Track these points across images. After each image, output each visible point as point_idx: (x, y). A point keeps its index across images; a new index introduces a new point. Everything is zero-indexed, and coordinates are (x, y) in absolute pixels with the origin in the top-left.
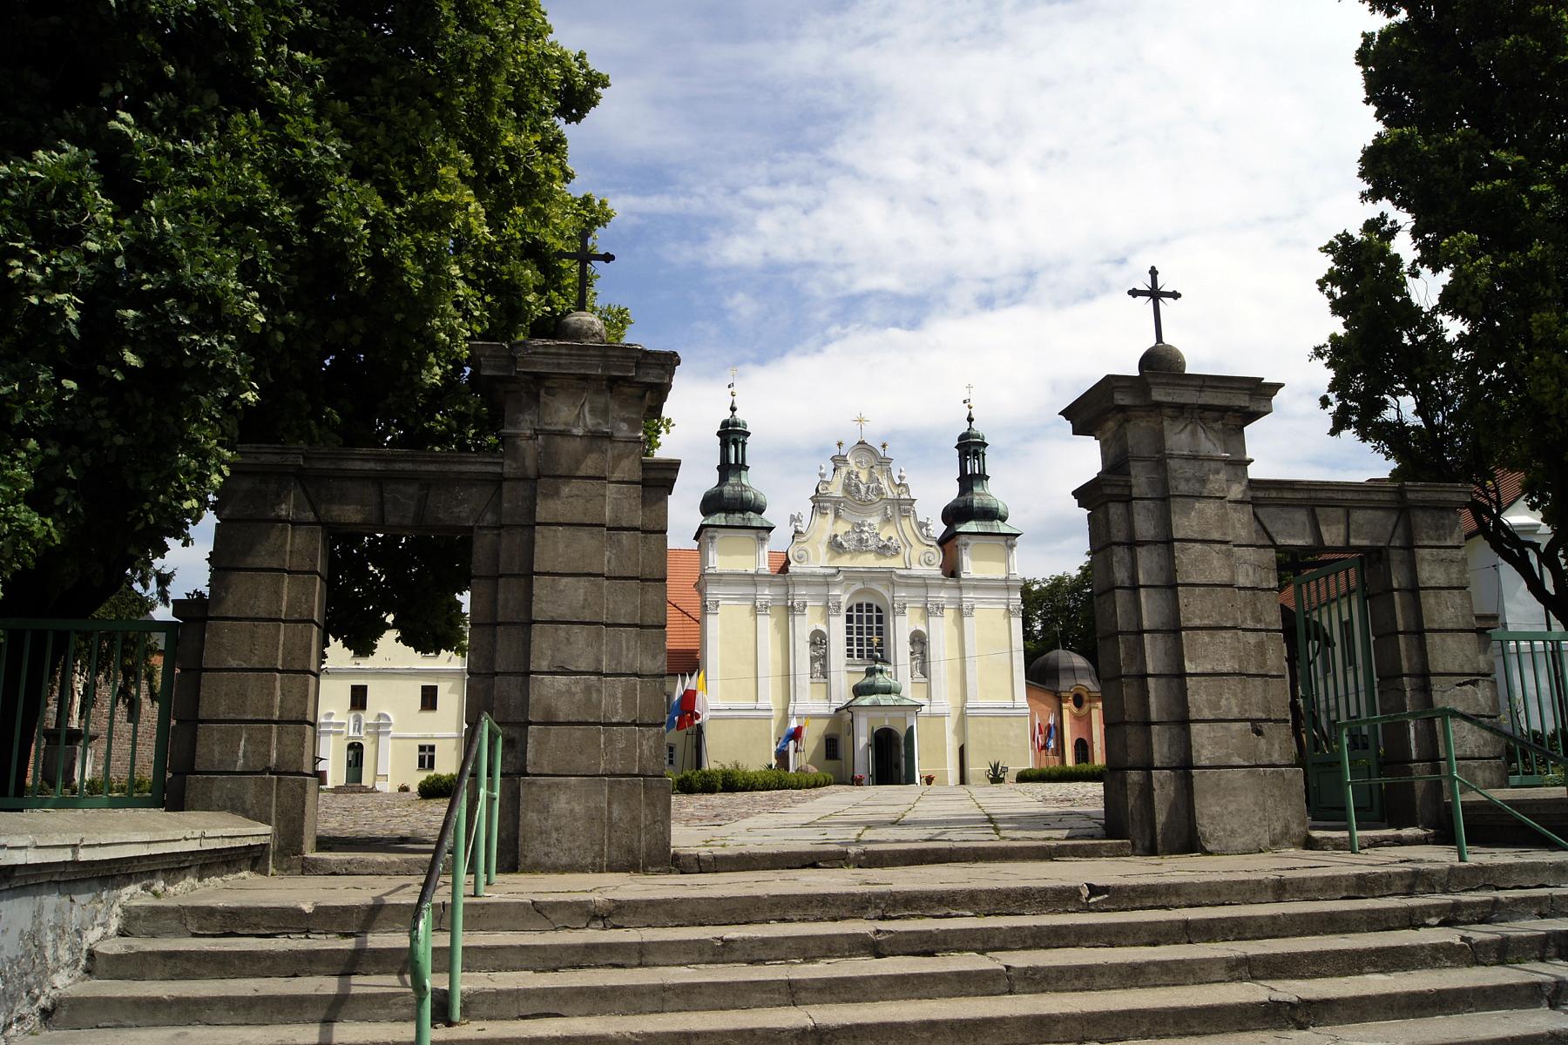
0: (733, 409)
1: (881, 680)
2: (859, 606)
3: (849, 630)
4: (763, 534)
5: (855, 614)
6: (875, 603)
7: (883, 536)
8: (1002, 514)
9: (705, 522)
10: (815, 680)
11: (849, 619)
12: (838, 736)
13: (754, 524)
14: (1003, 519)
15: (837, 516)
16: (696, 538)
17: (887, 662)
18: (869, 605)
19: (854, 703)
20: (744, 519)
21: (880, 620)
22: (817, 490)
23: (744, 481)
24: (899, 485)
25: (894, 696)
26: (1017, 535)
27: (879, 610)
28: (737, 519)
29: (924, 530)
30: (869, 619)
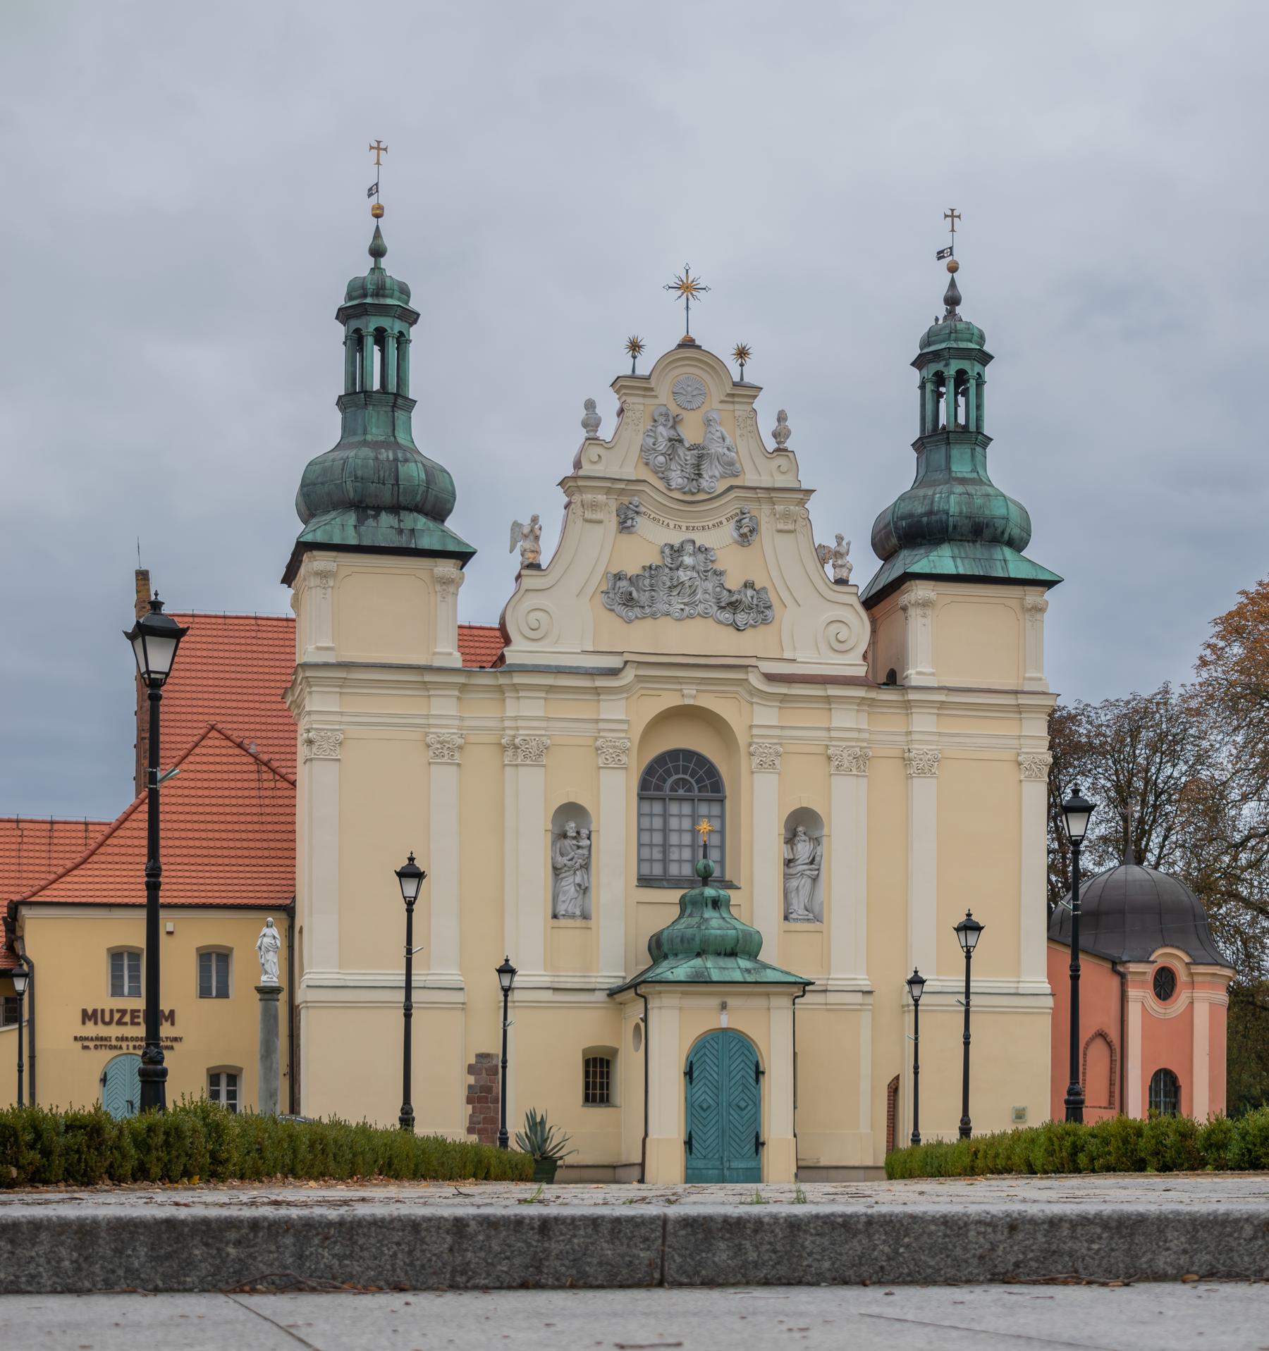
0: (377, 252)
1: (714, 923)
4: (446, 568)
7: (733, 582)
8: (1016, 532)
9: (309, 538)
10: (563, 922)
12: (614, 1052)
13: (426, 543)
14: (1017, 544)
15: (625, 525)
16: (289, 578)
17: (730, 886)
19: (650, 976)
20: (400, 531)
22: (578, 465)
23: (401, 438)
25: (744, 963)
26: (1049, 584)
29: (829, 569)
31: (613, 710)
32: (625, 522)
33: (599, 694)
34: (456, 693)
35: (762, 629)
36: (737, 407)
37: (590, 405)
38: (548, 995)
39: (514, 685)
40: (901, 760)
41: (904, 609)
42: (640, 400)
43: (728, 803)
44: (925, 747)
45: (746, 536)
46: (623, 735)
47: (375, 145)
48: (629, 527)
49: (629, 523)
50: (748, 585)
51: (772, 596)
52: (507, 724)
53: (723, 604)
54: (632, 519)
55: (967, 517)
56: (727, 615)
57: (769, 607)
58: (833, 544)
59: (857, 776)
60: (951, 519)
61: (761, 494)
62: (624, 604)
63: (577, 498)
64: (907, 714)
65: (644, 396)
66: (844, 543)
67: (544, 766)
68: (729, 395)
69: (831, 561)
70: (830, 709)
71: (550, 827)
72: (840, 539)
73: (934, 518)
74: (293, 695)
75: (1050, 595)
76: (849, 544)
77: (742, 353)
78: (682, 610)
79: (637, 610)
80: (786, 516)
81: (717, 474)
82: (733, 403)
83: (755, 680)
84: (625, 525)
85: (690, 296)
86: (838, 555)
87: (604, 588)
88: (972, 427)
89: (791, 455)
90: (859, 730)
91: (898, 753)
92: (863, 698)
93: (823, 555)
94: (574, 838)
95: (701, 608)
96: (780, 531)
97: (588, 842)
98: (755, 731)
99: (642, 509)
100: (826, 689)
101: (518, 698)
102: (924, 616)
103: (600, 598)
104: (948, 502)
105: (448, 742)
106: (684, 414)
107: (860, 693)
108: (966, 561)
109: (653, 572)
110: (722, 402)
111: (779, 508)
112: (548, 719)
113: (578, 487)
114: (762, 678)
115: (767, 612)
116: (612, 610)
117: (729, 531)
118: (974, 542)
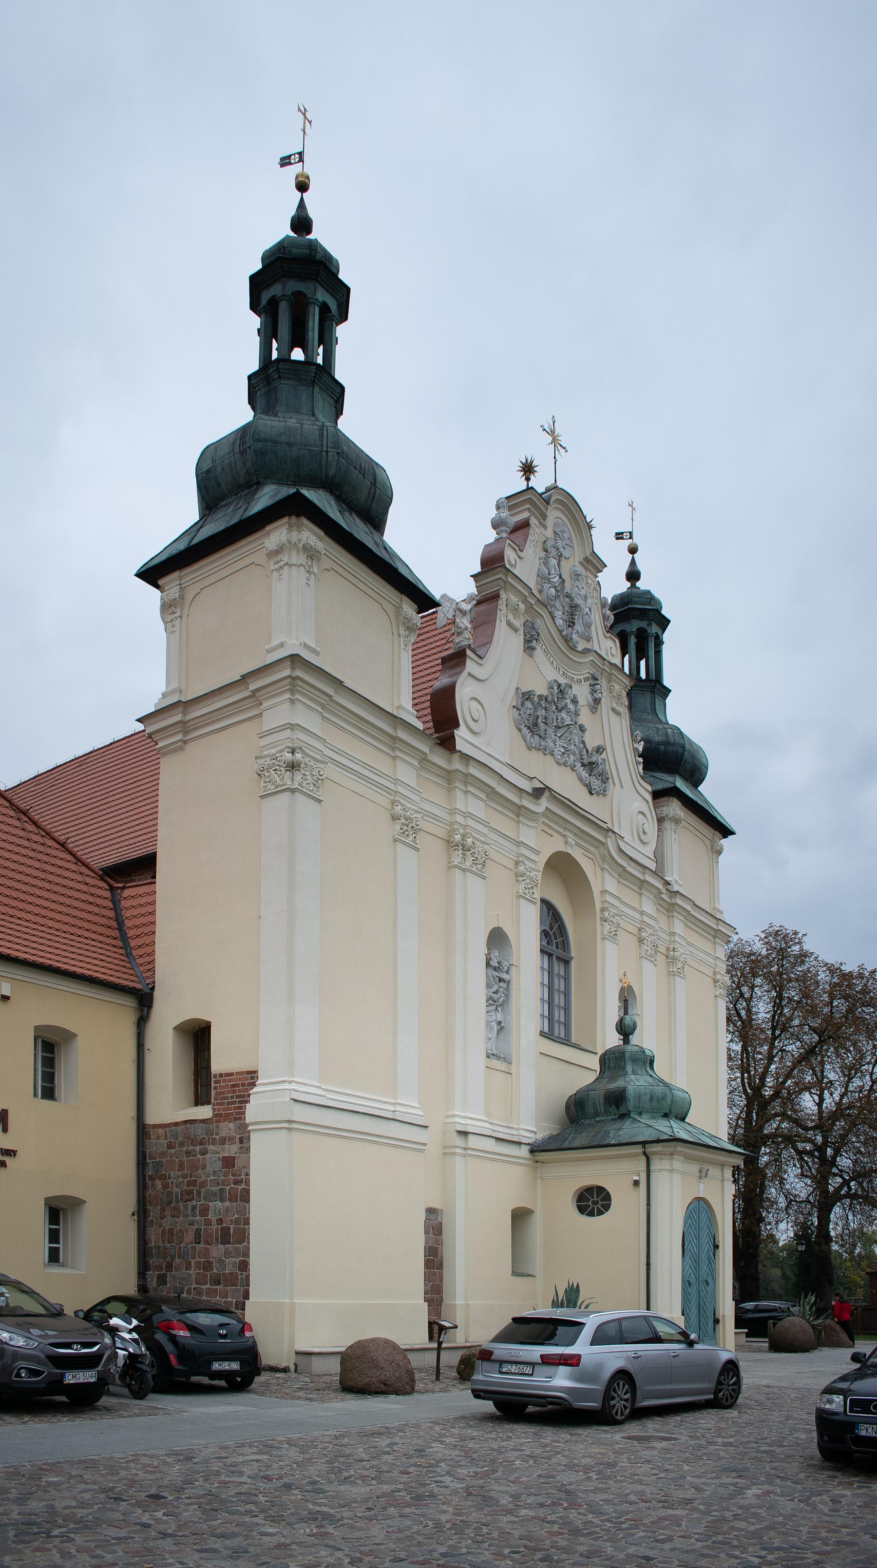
38: (491, 1145)
39: (468, 775)
43: (573, 964)
50: (599, 750)
60: (686, 753)
64: (669, 917)
70: (641, 894)
74: (185, 714)
75: (724, 841)
96: (613, 710)
116: (520, 730)
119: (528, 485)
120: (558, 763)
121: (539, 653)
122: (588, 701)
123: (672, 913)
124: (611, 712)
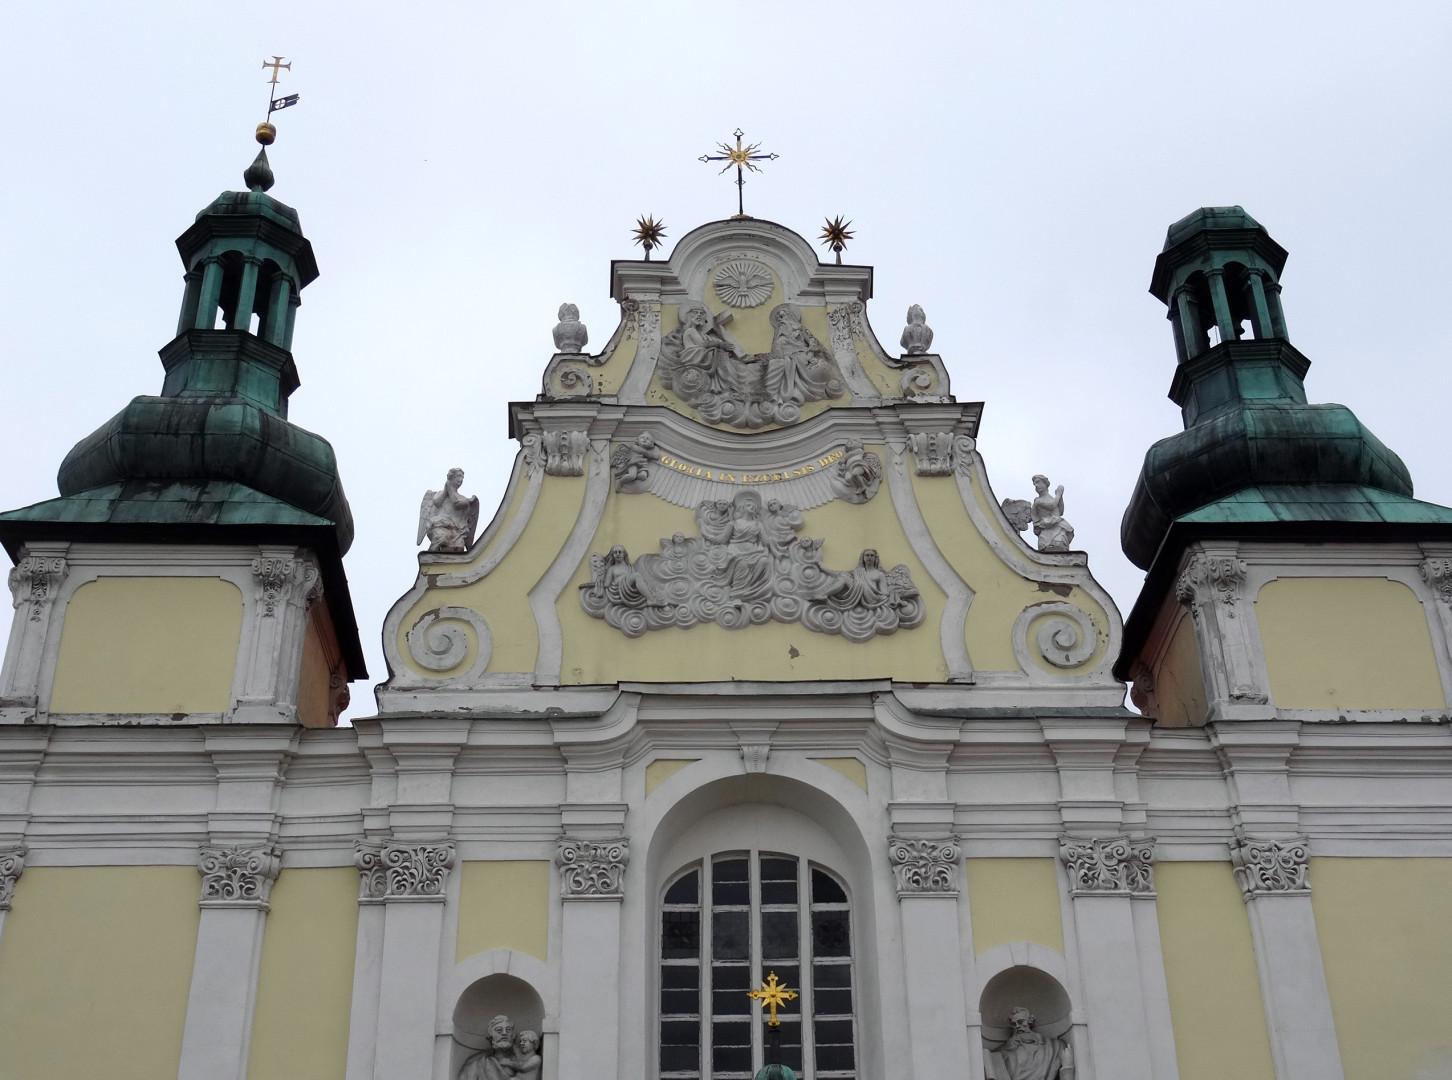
2: (730, 873)
3: (677, 991)
5: (706, 908)
6: (806, 847)
7: (841, 559)
11: (678, 934)
15: (627, 480)
18: (779, 869)
21: (833, 934)
24: (902, 364)
27: (826, 887)
28: (170, 505)
30: (781, 935)
31: (591, 787)
32: (626, 472)
33: (565, 760)
34: (274, 773)
35: (903, 638)
36: (828, 298)
37: (569, 312)
39: (387, 747)
40: (1224, 875)
41: (1188, 600)
42: (655, 297)
44: (1274, 837)
45: (861, 484)
46: (616, 834)
47: (274, 61)
48: (632, 481)
49: (633, 472)
50: (870, 561)
51: (920, 584)
52: (370, 823)
53: (820, 597)
54: (639, 467)
55: (1281, 439)
56: (828, 615)
57: (913, 598)
58: (1030, 495)
59: (1132, 898)
60: (1251, 444)
61: (886, 418)
62: (623, 605)
63: (533, 439)
65: (662, 293)
66: (1051, 491)
67: (443, 902)
68: (815, 282)
69: (1031, 526)
71: (448, 1027)
72: (1041, 483)
73: (1219, 450)
76: (1060, 491)
77: (836, 234)
78: (738, 608)
79: (649, 615)
80: (931, 450)
81: (797, 394)
82: (823, 294)
83: (886, 716)
84: (627, 480)
85: (744, 167)
86: (1041, 509)
87: (585, 580)
88: (1268, 333)
89: (933, 360)
90: (1124, 807)
91: (1216, 853)
92: (1123, 744)
93: (1013, 515)
94: (509, 1052)
95: (776, 606)
96: (923, 474)
97: (535, 1059)
98: (899, 817)
99: (656, 452)
100: (1041, 730)
101: (396, 774)
102: (1228, 602)
103: (575, 598)
104: (1242, 419)
105: (244, 865)
106: (737, 314)
107: (1117, 734)
108: (1293, 507)
109: (679, 549)
110: (803, 294)
111: (920, 438)
112: (456, 810)
113: (536, 420)
114: (909, 717)
115: (909, 607)
116: (602, 617)
117: (829, 484)
118: (1304, 483)
119: (647, 256)
120: (731, 627)
121: (657, 477)
122: (834, 489)
123: (1230, 765)
124: (917, 481)
